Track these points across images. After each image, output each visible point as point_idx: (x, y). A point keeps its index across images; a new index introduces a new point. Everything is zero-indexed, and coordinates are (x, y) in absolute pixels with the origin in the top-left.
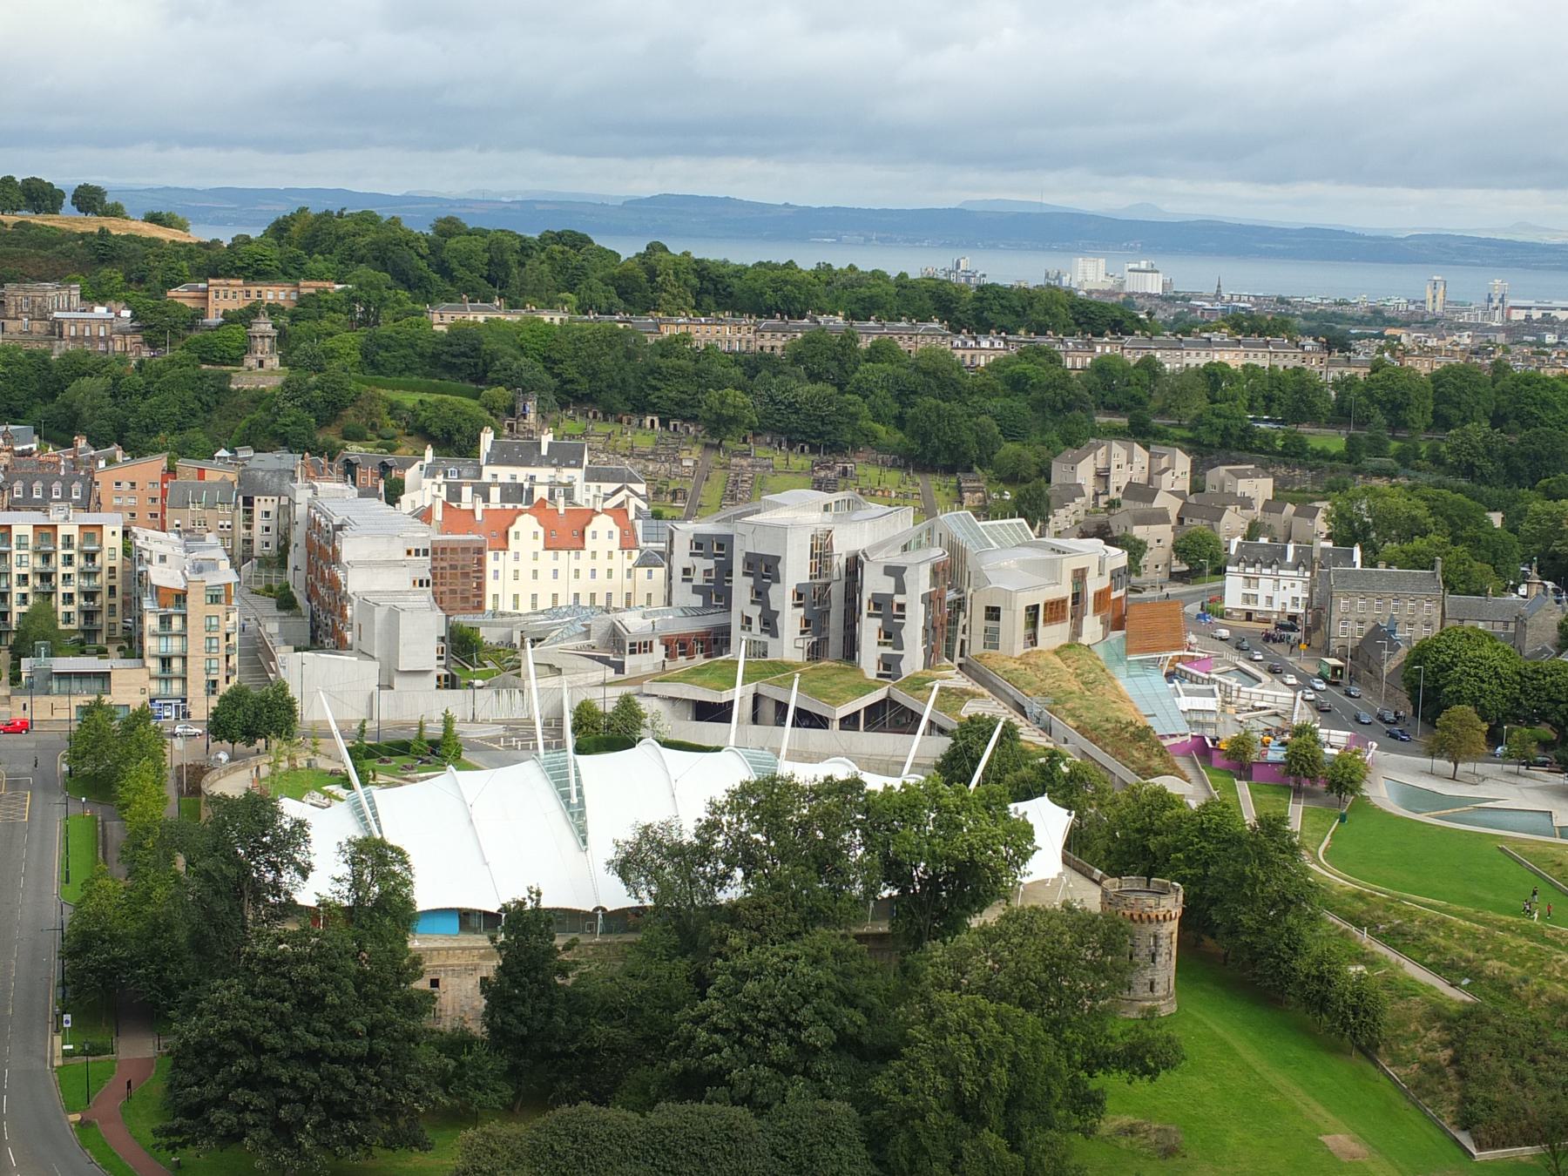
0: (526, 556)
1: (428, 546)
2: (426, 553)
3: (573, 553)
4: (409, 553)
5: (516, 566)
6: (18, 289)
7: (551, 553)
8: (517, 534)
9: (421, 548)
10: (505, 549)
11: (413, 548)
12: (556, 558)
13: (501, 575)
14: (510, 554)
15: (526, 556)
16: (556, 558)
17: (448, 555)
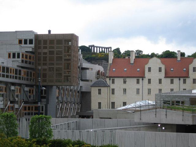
0: (155, 82)
1: (32, 37)
2: (31, 42)
3: (182, 80)
4: (20, 42)
5: (149, 86)
6: (95, 62)
7: (169, 80)
8: (150, 69)
9: (28, 38)
10: (143, 77)
11: (23, 38)
12: (172, 82)
13: (141, 91)
14: (146, 80)
15: (155, 82)
16: (172, 82)
17: (48, 45)
